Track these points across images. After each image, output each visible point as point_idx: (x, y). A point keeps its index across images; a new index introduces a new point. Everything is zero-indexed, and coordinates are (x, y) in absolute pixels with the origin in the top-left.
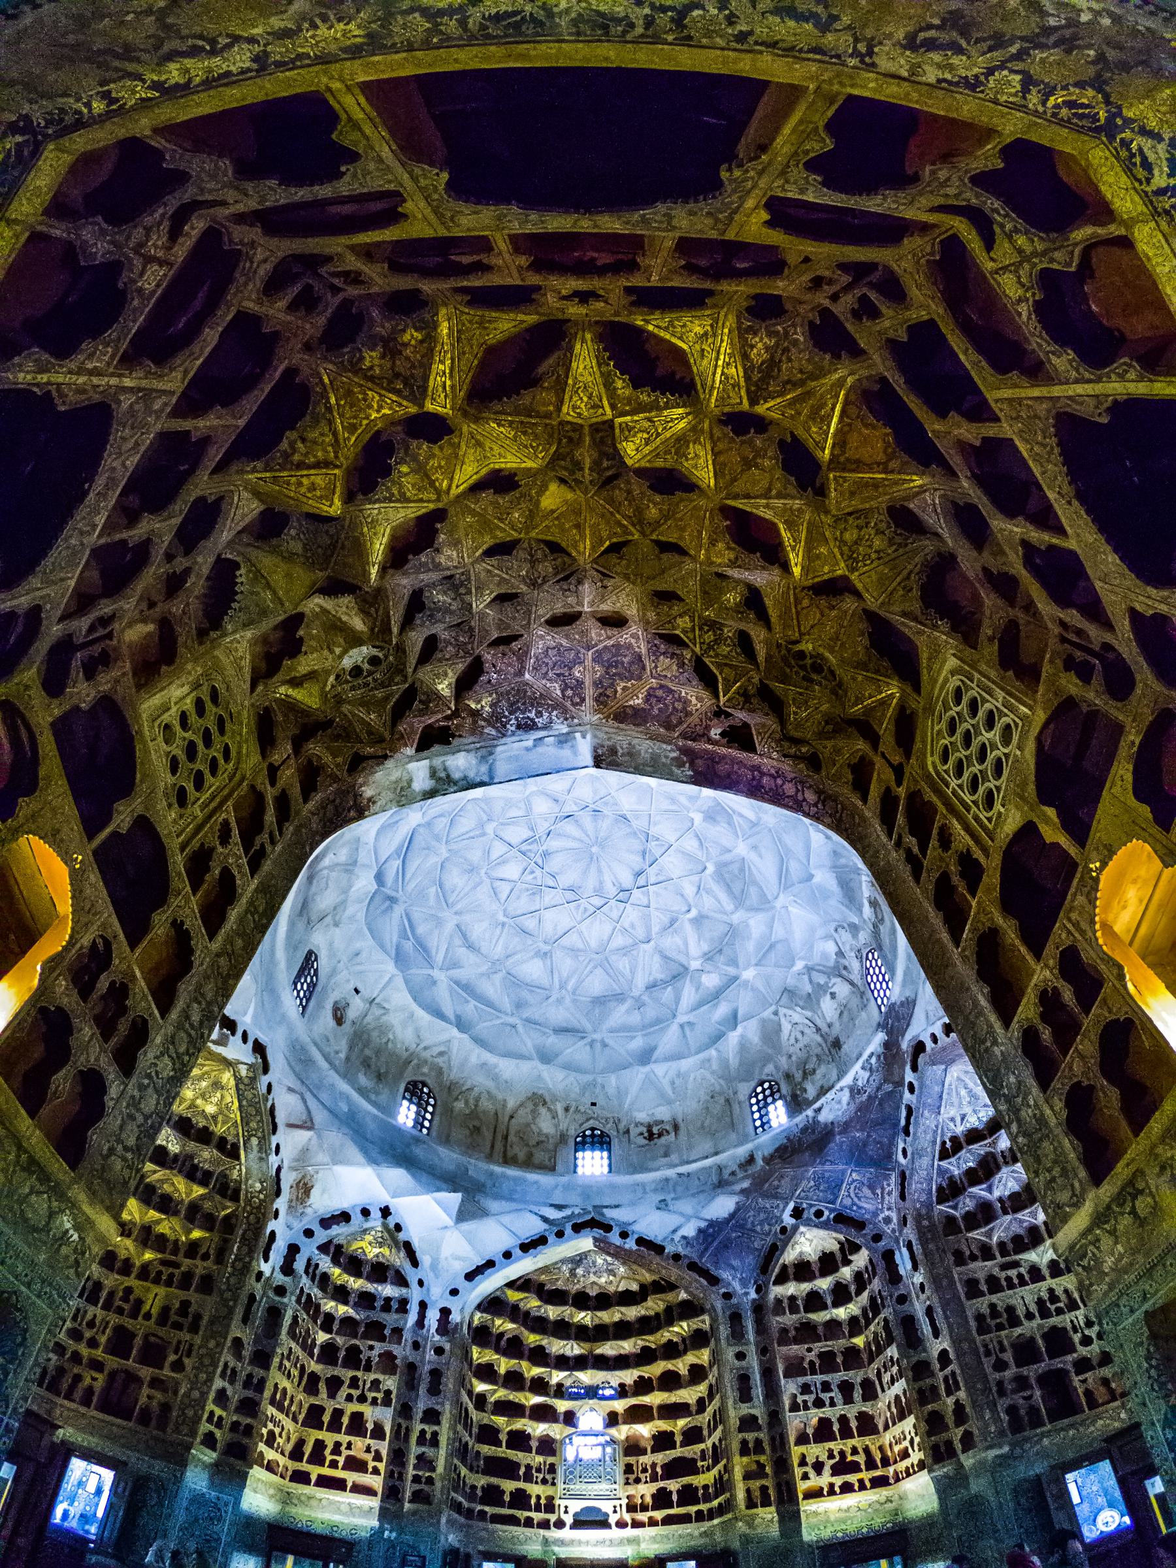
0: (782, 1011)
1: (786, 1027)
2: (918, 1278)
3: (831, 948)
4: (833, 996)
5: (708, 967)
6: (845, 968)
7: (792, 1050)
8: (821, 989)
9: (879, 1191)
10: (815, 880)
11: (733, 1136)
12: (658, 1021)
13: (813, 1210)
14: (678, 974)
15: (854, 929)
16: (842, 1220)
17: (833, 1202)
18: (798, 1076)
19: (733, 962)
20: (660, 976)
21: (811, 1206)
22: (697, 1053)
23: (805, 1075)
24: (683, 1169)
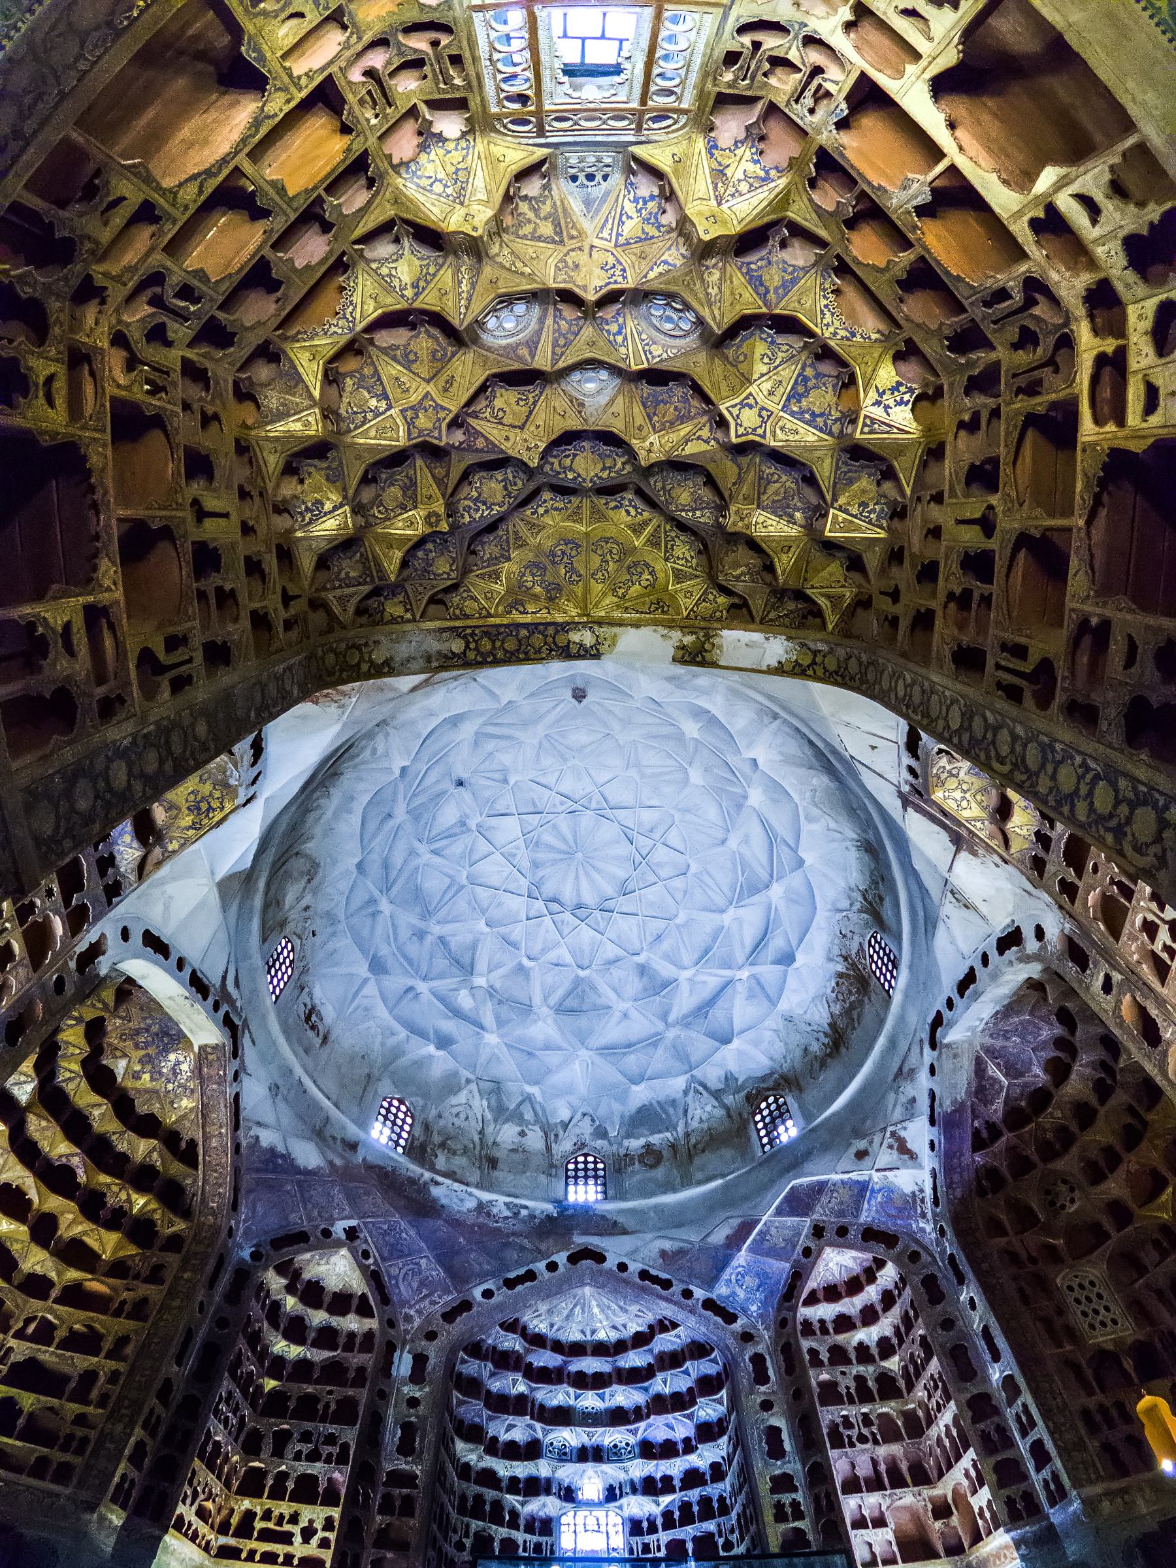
0: (473, 1086)
1: (462, 1098)
2: (409, 1390)
3: (565, 1114)
4: (522, 1134)
5: (480, 994)
6: (556, 1136)
7: (446, 1114)
8: (516, 1116)
9: (425, 1292)
10: (634, 1088)
11: (355, 1110)
12: (410, 962)
13: (364, 1247)
14: (465, 967)
15: (601, 1133)
16: (374, 1278)
17: (384, 1259)
18: (437, 1139)
19: (501, 1022)
20: (452, 946)
21: (366, 1241)
22: (398, 1019)
23: (443, 1145)
24: (308, 1082)
